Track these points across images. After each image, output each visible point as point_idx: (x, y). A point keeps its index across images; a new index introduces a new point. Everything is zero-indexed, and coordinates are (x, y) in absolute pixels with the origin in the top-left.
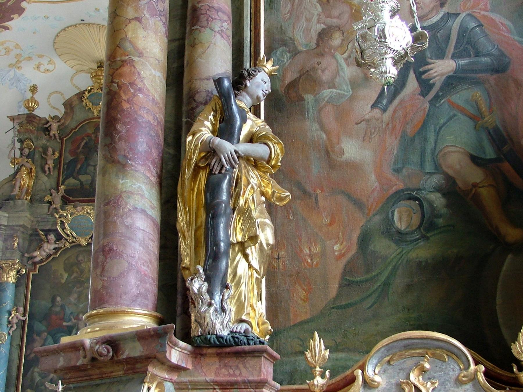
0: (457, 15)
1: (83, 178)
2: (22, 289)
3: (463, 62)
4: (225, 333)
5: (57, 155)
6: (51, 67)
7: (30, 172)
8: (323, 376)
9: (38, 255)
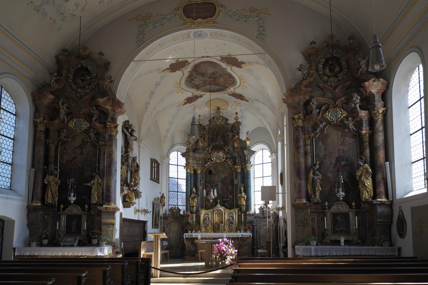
0: (345, 155)
1: (216, 143)
2: (202, 174)
3: (346, 162)
4: (316, 202)
5: (208, 136)
6: (203, 109)
7: (202, 142)
8: (327, 207)
9: (206, 165)
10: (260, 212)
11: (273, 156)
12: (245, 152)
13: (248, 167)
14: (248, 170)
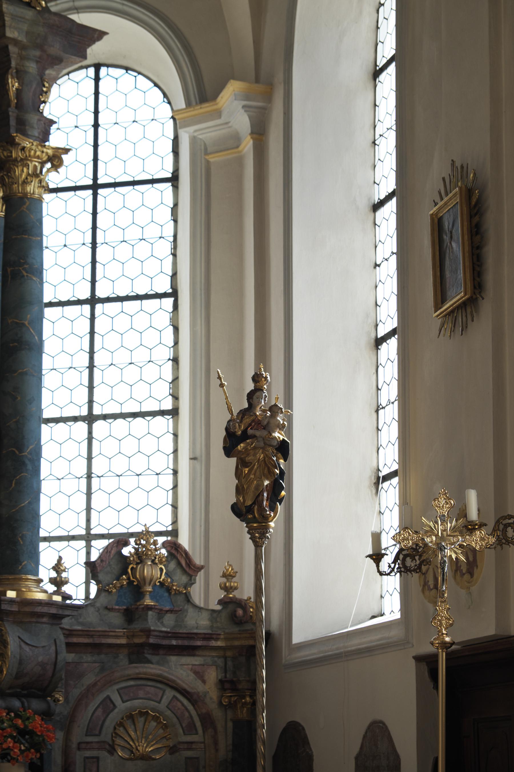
10: (104, 600)
11: (218, 114)
12: (14, 17)
13: (24, 162)
14: (25, 197)
